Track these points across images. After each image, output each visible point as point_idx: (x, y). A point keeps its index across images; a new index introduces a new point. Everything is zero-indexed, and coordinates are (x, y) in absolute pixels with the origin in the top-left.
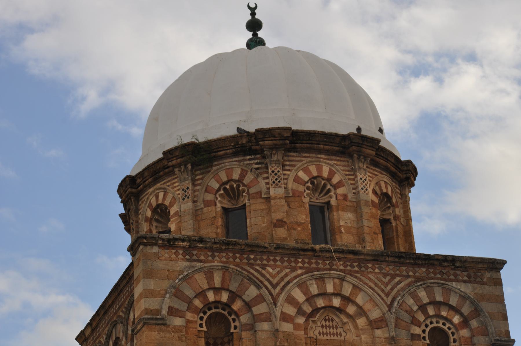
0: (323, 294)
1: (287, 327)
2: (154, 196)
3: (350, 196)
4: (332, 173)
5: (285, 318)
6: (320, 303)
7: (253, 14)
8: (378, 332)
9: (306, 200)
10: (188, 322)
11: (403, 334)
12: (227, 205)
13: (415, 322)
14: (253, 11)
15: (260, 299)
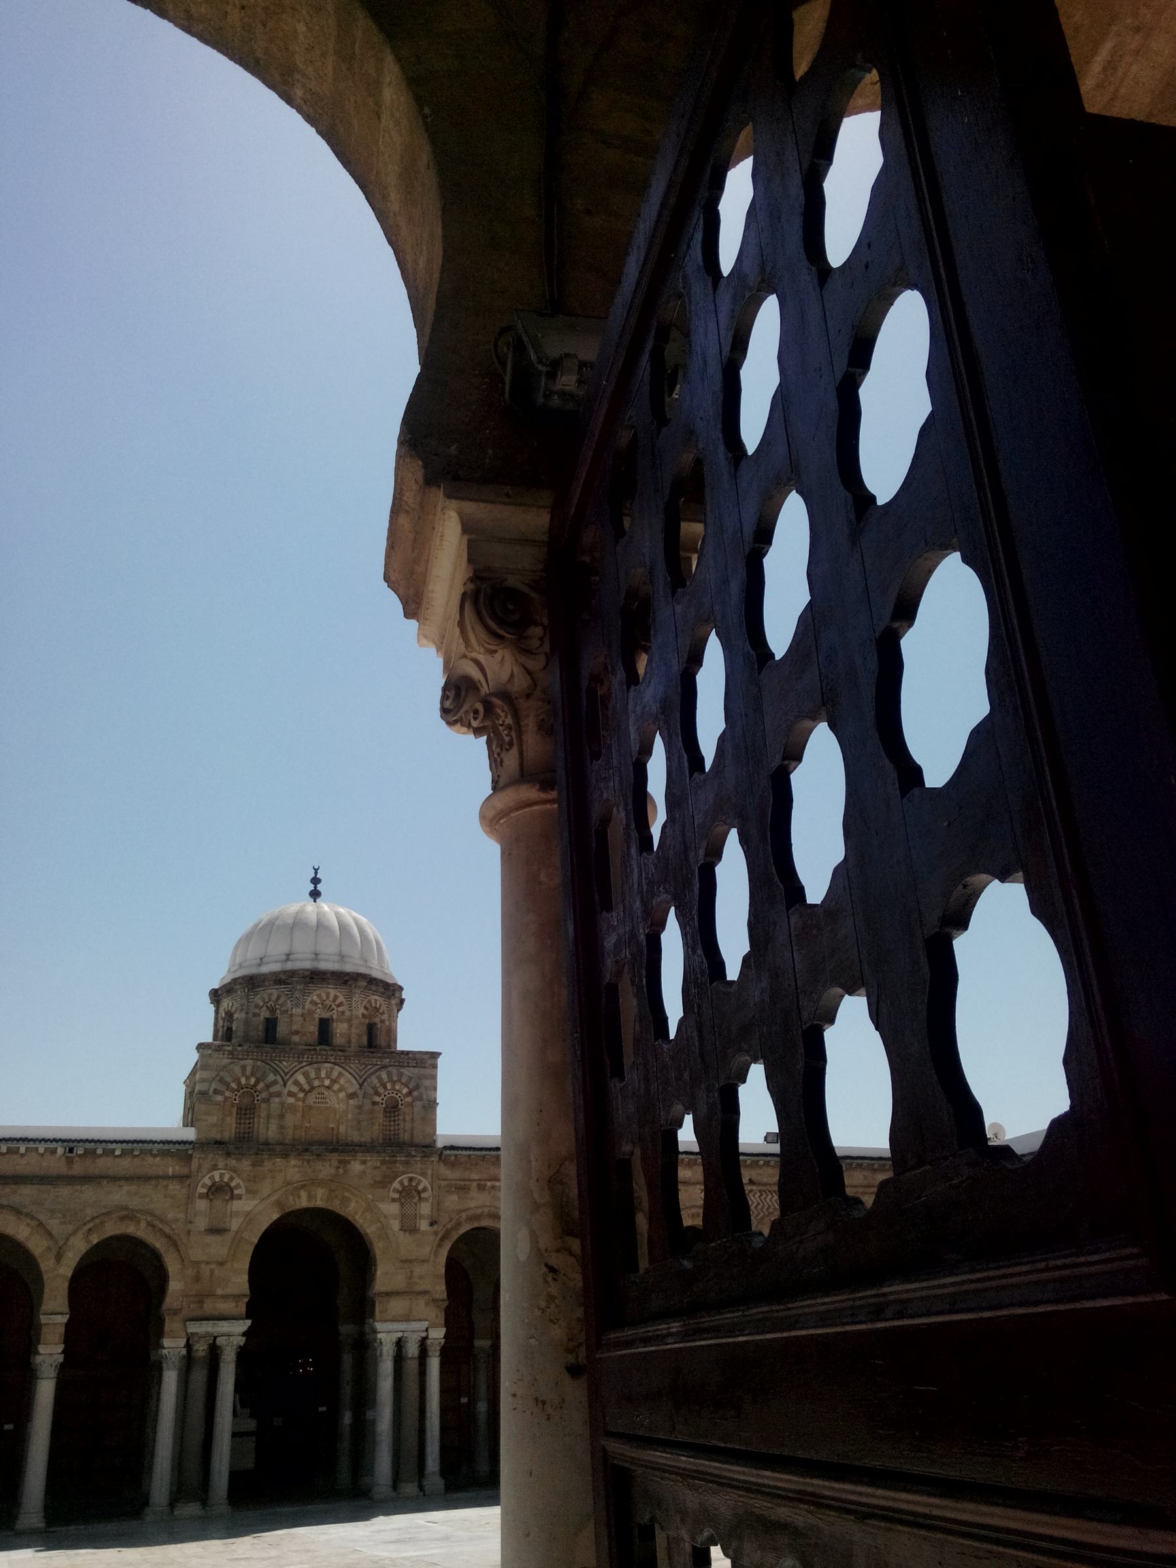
0: (318, 1077)
1: (291, 1100)
2: (226, 1003)
3: (348, 1013)
4: (336, 997)
5: (291, 1094)
6: (316, 1083)
7: (316, 873)
8: (351, 1102)
9: (316, 1016)
10: (226, 1098)
11: (367, 1101)
12: (268, 1015)
13: (377, 1094)
14: (316, 870)
15: (275, 1082)
